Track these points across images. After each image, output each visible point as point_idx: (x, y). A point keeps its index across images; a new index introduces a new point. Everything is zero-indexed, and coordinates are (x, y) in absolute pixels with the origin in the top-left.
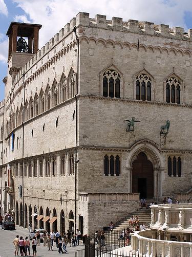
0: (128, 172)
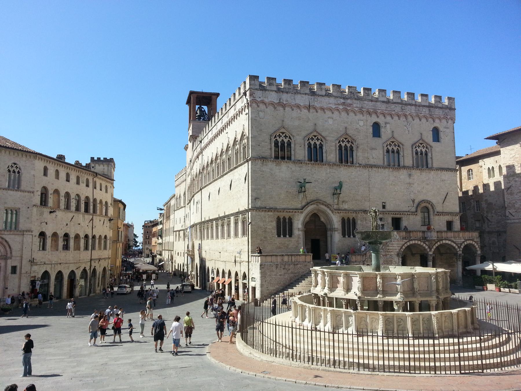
0: (301, 233)
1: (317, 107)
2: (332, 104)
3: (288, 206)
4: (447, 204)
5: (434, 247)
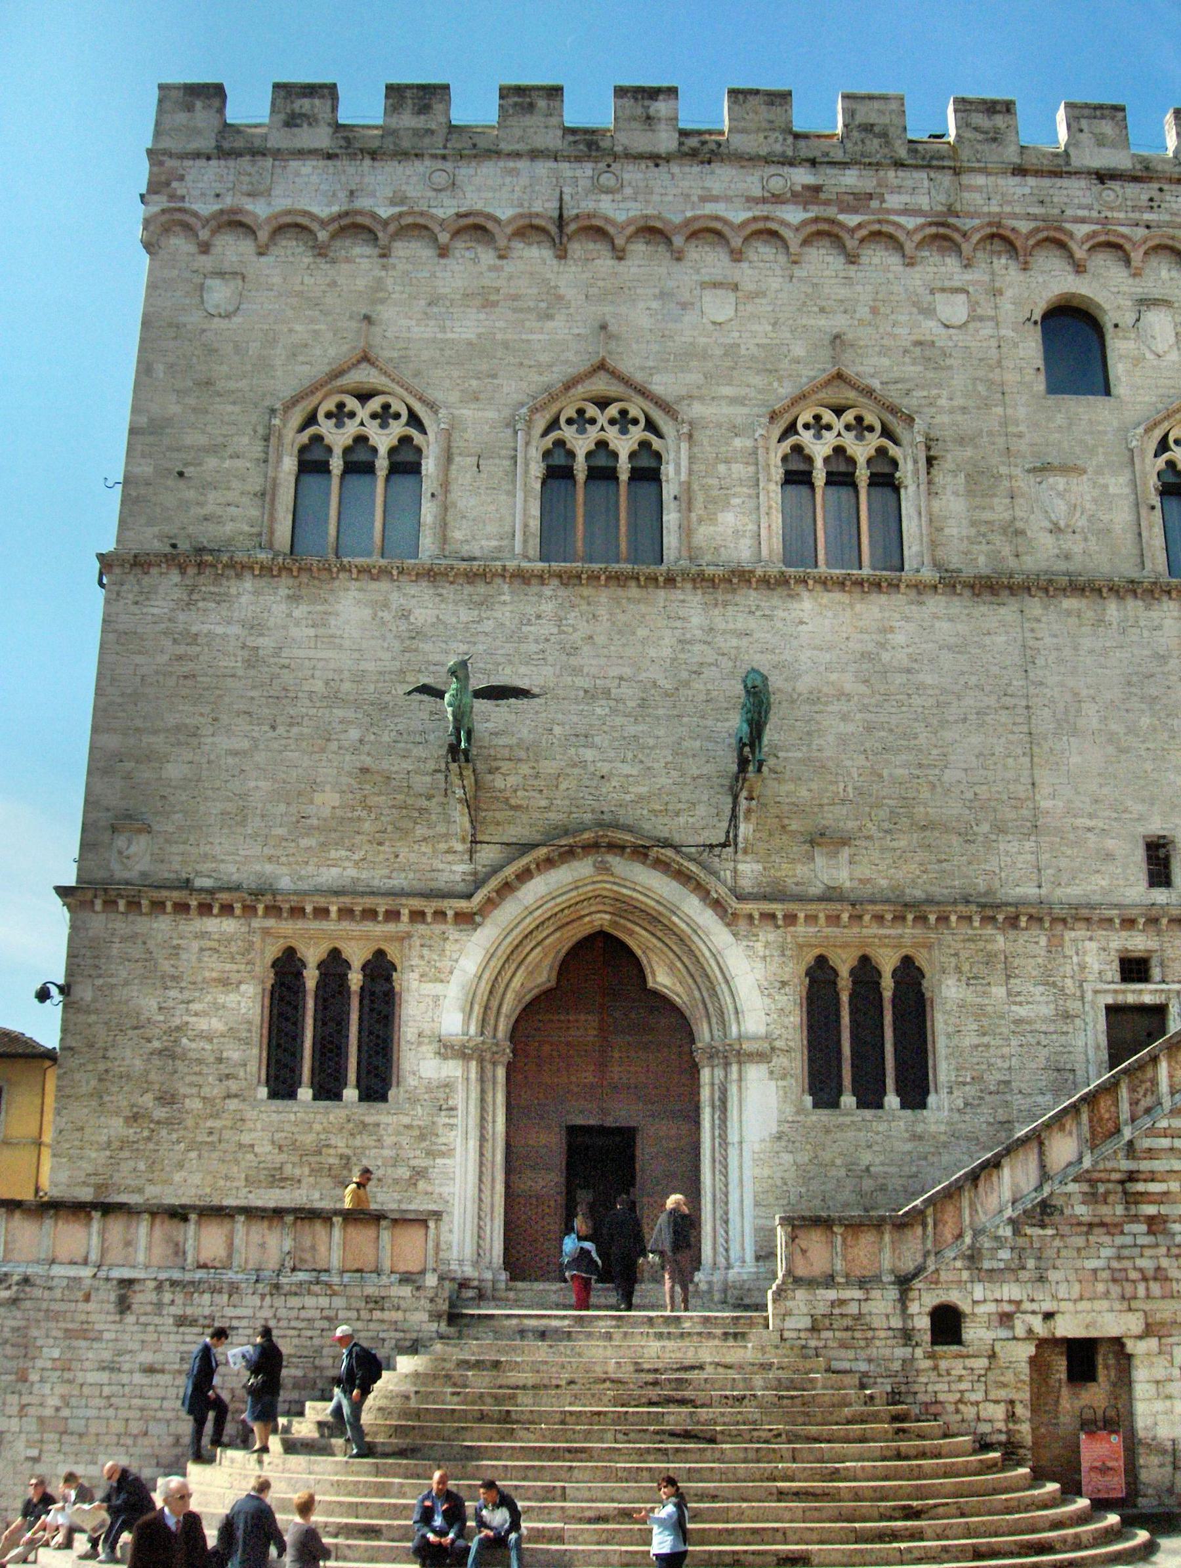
2: (728, 199)
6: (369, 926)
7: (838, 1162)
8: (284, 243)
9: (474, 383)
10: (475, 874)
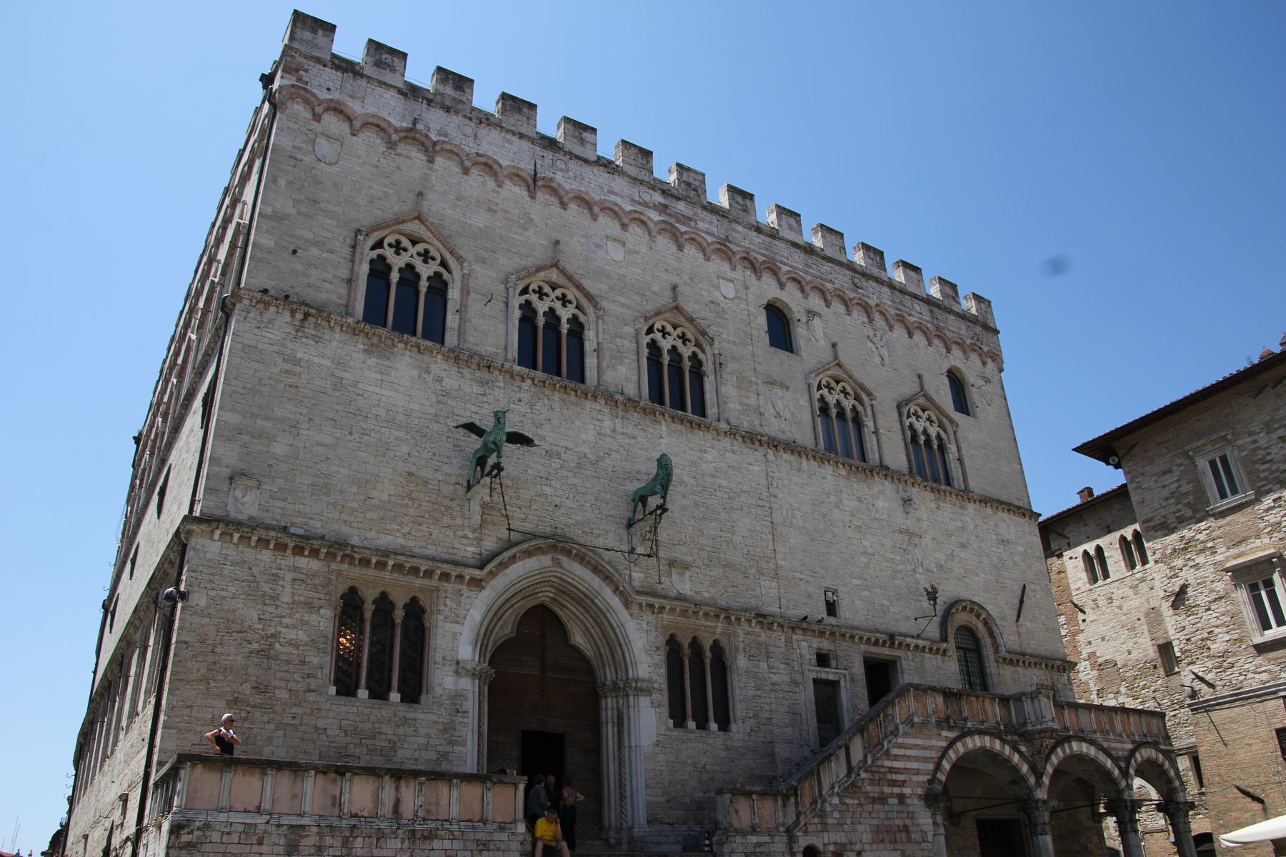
0: (468, 686)
1: (564, 189)
2: (622, 196)
3: (409, 544)
4: (1028, 624)
5: (1050, 769)
6: (411, 578)
7: (689, 762)
8: (369, 134)
9: (483, 252)
10: (481, 554)
